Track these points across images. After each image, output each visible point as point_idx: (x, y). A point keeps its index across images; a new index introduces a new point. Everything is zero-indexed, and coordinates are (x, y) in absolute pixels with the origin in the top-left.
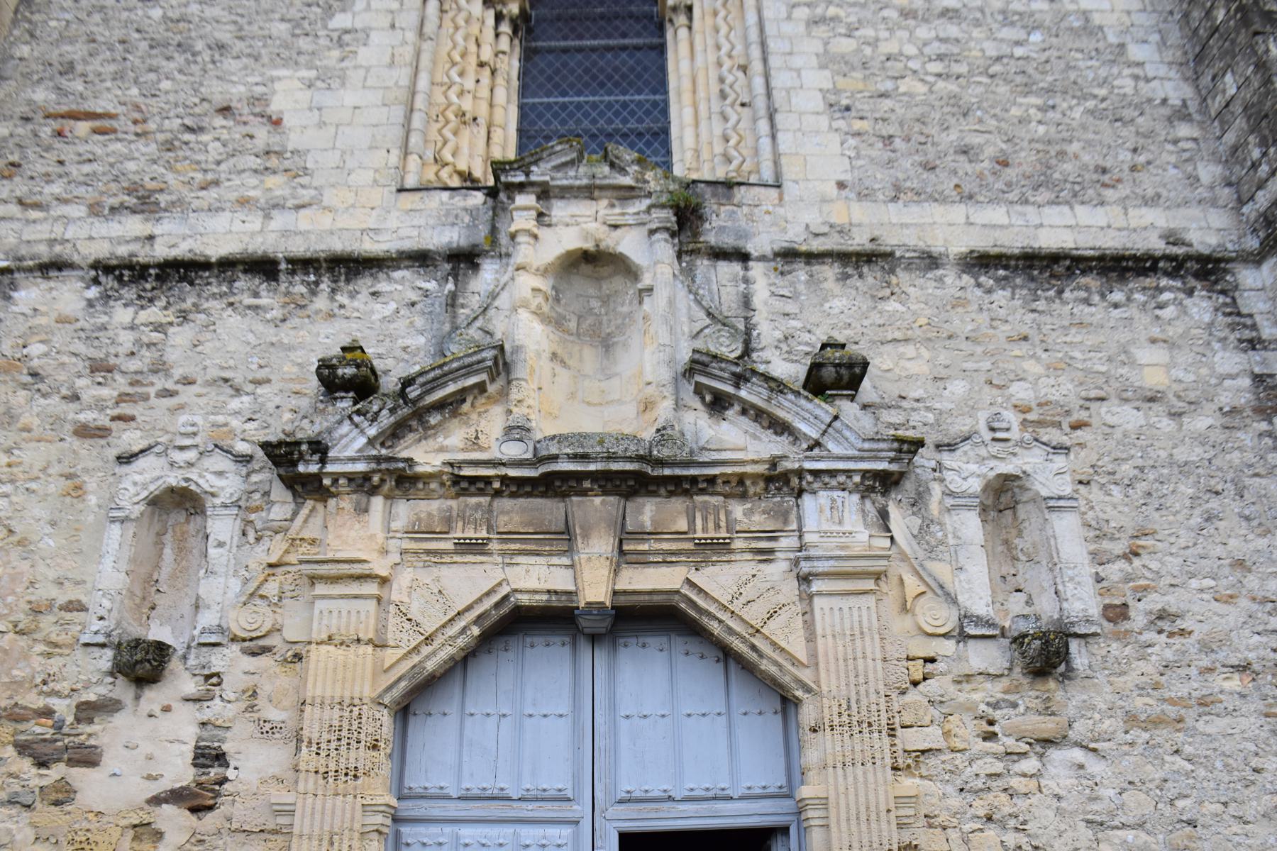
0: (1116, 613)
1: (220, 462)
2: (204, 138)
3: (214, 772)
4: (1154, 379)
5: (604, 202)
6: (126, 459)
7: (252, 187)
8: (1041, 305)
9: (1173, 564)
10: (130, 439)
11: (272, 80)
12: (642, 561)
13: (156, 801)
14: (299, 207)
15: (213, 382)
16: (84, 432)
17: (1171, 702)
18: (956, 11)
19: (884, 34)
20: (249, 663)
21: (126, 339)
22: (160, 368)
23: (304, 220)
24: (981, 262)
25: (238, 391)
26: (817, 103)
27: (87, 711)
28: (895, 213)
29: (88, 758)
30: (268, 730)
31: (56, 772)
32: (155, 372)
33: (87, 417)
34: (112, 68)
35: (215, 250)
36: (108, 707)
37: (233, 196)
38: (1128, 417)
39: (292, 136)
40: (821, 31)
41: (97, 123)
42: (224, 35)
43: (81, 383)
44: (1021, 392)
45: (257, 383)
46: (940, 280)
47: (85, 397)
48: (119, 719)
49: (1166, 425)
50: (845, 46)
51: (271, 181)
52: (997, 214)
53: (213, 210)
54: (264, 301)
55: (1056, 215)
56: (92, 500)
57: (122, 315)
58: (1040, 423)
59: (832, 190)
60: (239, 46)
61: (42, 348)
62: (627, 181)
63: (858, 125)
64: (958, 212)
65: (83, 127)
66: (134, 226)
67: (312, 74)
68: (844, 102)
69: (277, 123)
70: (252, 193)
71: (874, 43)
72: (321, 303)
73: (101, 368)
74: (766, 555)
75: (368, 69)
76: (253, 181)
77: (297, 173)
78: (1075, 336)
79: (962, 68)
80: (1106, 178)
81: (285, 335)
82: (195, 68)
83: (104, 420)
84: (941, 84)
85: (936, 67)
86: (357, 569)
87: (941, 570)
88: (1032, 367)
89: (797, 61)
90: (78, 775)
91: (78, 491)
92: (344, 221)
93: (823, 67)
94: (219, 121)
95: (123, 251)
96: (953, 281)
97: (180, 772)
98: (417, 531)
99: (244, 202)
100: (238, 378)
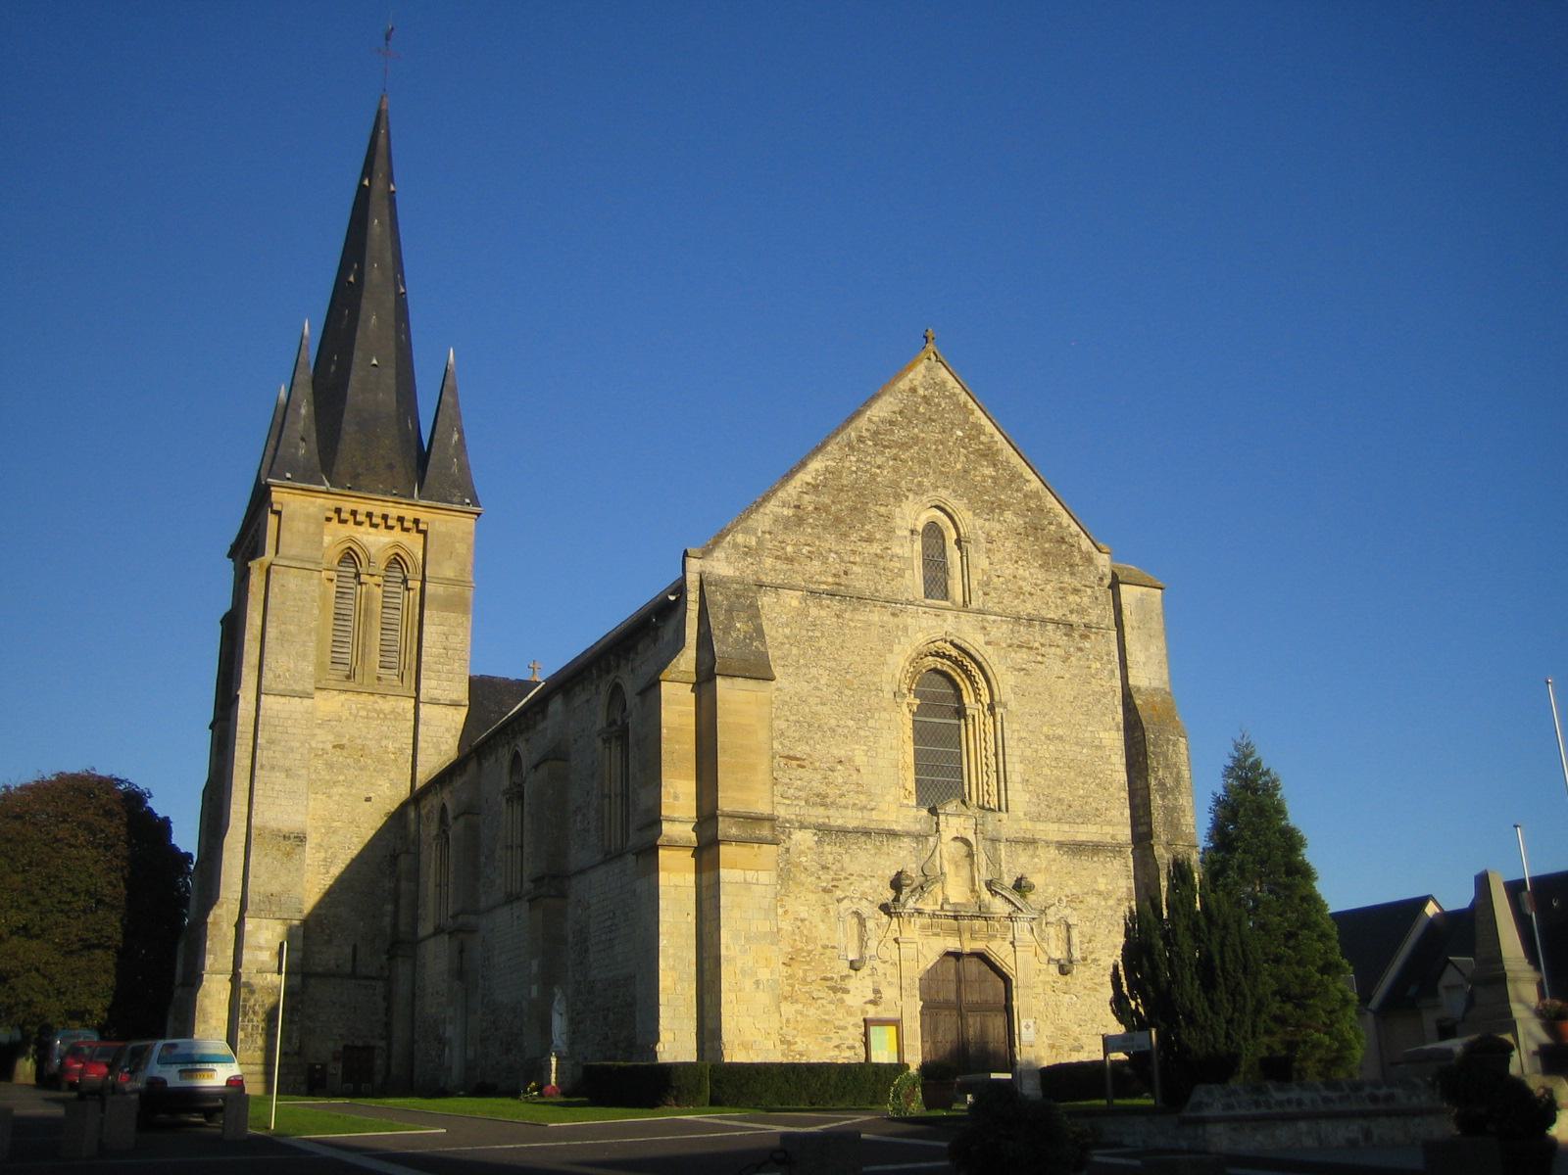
0: (1084, 959)
1: (864, 902)
2: (835, 774)
3: (878, 995)
4: (1102, 887)
5: (962, 819)
6: (839, 901)
7: (852, 798)
8: (1075, 861)
9: (1099, 945)
10: (839, 893)
11: (854, 749)
12: (976, 939)
13: (866, 1003)
14: (872, 809)
15: (858, 876)
16: (825, 890)
17: (1095, 984)
18: (1062, 737)
19: (1040, 747)
20: (882, 965)
21: (830, 858)
22: (842, 869)
23: (874, 815)
24: (1060, 845)
25: (866, 879)
26: (1019, 779)
27: (843, 978)
28: (1040, 826)
29: (847, 991)
30: (890, 984)
31: (839, 995)
32: (842, 870)
33: (824, 884)
34: (797, 735)
35: (851, 825)
36: (848, 976)
37: (851, 802)
38: (1093, 900)
39: (865, 777)
40: (1021, 745)
41: (798, 762)
42: (833, 722)
43: (820, 873)
44: (1067, 891)
45: (871, 876)
46: (1049, 851)
47: (822, 877)
48: (852, 981)
49: (1103, 903)
50: (1028, 752)
51: (862, 797)
52: (1066, 827)
53: (846, 808)
54: (869, 847)
55: (1083, 828)
56: (832, 914)
57: (828, 848)
58: (1071, 901)
59: (1021, 814)
60: (840, 730)
61: (805, 859)
62: (970, 813)
63: (1031, 788)
64: (1055, 826)
65: (794, 763)
66: (821, 810)
67: (865, 748)
68: (1027, 778)
69: (858, 771)
70: (857, 802)
71: (1036, 751)
72: (885, 849)
73: (825, 868)
74: (1004, 939)
75: (884, 749)
76: (855, 796)
77: (869, 794)
78: (1084, 873)
79: (1061, 764)
80: (1097, 813)
81: (877, 859)
82: (826, 740)
83: (830, 886)
84: (1055, 772)
85: (1054, 764)
86: (911, 940)
87: (1045, 945)
88: (1071, 883)
89: (1014, 759)
90: (845, 996)
91: (827, 911)
92: (886, 817)
93: (1021, 762)
94: (839, 767)
95: (820, 821)
96: (1053, 852)
97: (871, 996)
98: (923, 927)
99: (854, 804)
100: (866, 874)
